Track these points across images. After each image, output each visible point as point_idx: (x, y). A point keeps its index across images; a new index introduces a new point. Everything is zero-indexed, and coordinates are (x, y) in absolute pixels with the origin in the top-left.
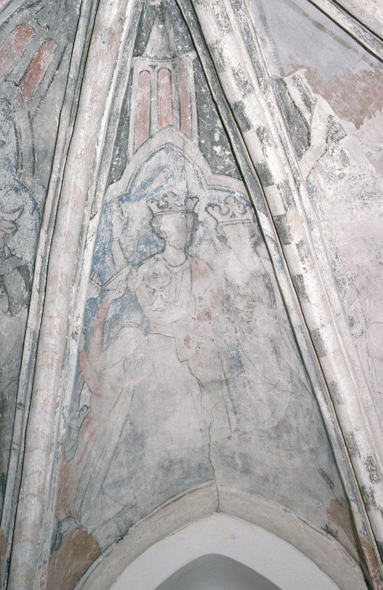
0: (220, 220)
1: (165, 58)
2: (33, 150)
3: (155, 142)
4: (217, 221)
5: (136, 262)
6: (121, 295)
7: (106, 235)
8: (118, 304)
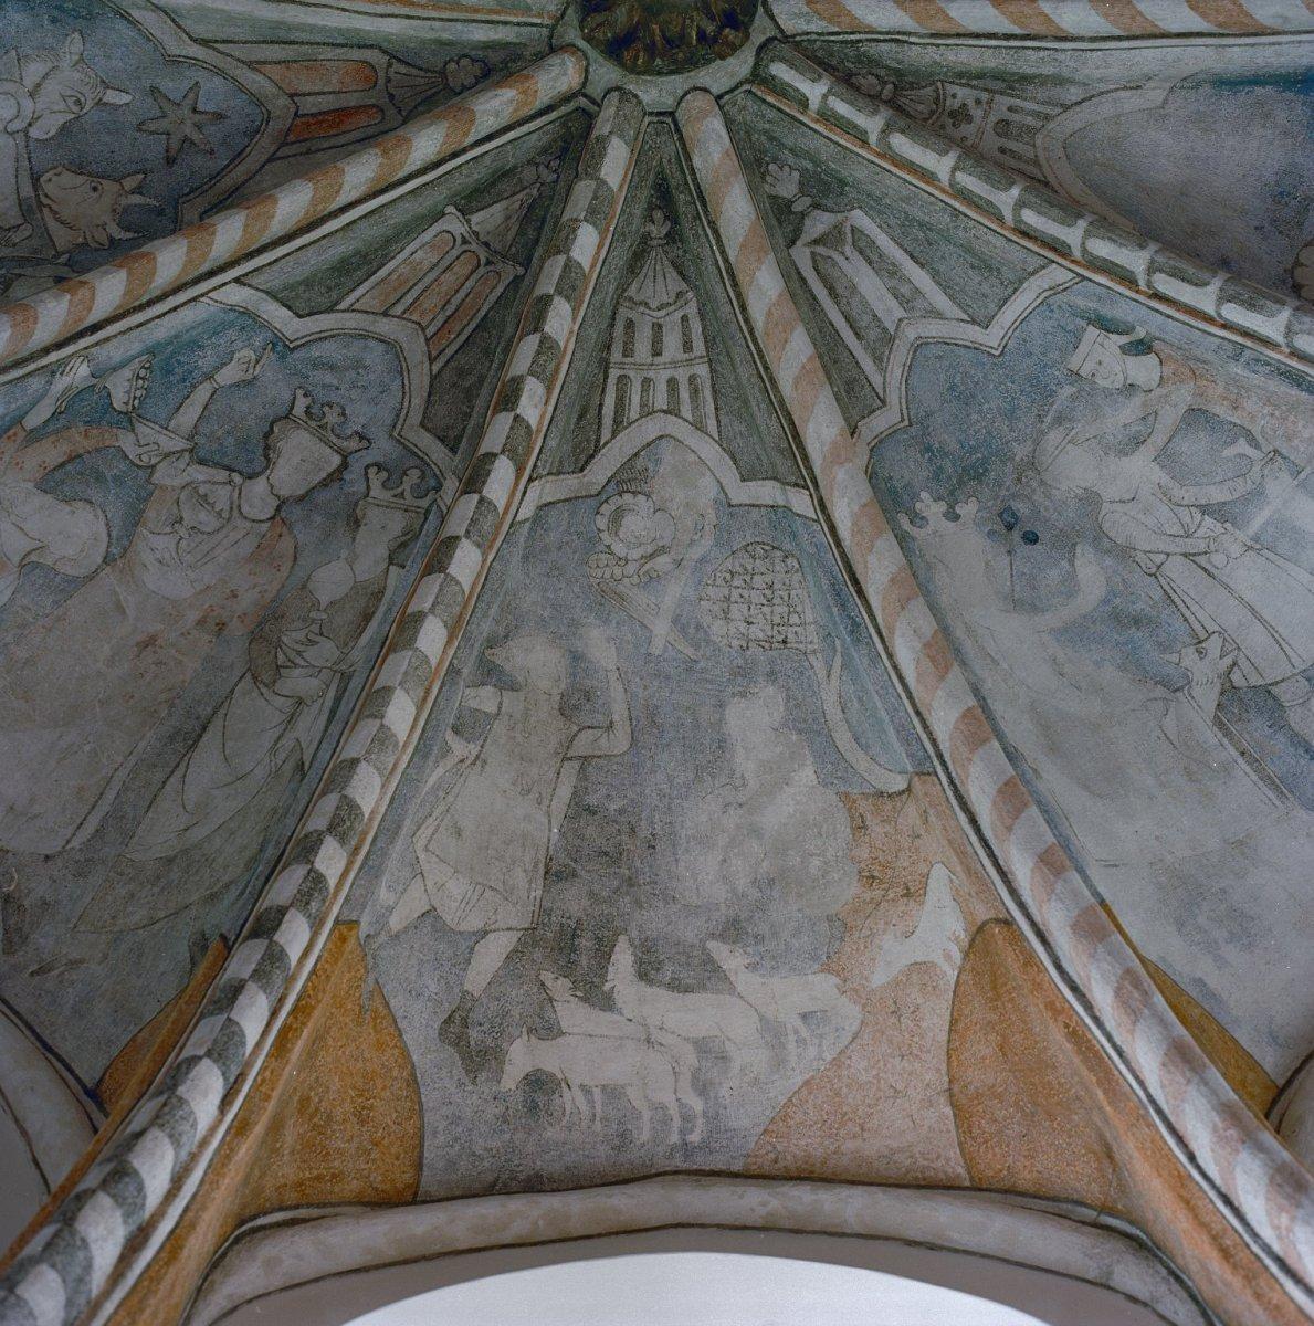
0: (372, 493)
1: (486, 244)
3: (385, 327)
4: (368, 495)
5: (202, 454)
6: (137, 461)
7: (206, 360)
8: (122, 466)
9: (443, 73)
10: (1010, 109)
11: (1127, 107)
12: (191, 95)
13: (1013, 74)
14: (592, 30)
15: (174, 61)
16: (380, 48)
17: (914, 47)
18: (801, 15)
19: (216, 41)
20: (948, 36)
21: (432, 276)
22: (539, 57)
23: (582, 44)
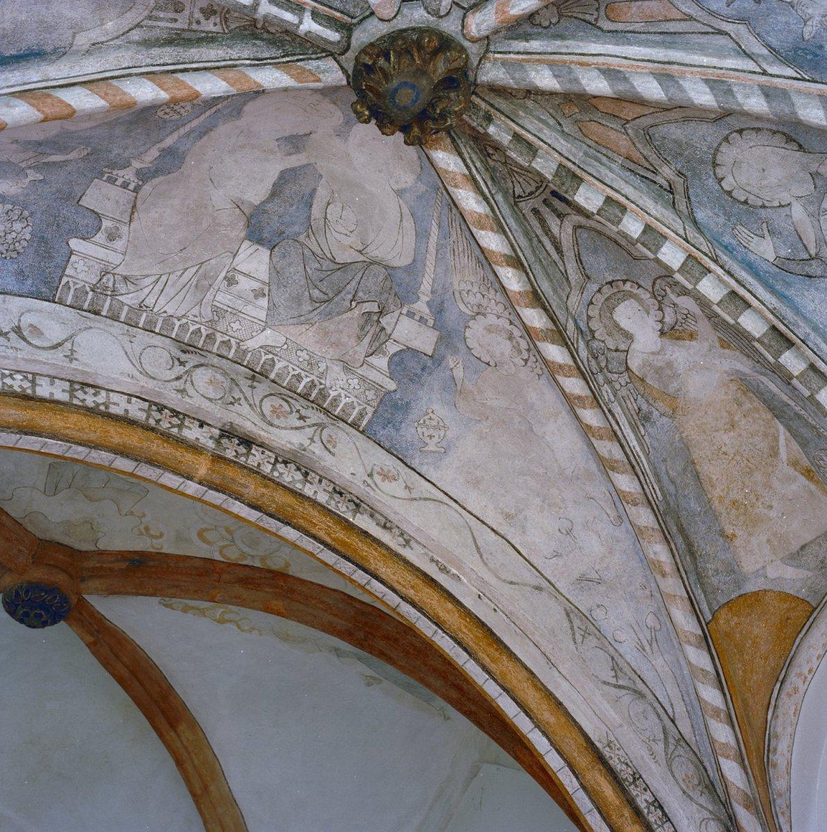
9: (560, 16)
10: (176, 20)
11: (98, 31)
13: (178, 45)
14: (460, 57)
15: (742, 20)
16: (602, 30)
17: (246, 57)
18: (323, 72)
19: (713, 33)
20: (224, 67)
22: (496, 32)
23: (466, 44)
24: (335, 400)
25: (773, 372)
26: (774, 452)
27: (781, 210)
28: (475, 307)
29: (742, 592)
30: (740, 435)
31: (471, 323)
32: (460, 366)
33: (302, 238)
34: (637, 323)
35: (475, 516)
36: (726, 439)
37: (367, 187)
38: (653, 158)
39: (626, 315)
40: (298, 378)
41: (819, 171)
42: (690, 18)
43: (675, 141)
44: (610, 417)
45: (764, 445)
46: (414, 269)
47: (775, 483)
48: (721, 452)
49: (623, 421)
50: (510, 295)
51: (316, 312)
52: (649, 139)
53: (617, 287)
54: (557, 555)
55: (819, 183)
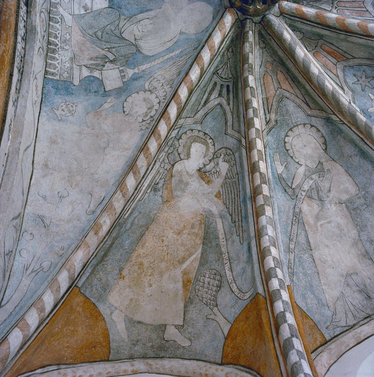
1: (332, 3)
2: (368, 59)
12: (356, 83)
15: (352, 91)
19: (340, 86)
21: (349, 8)
24: (54, 58)
25: (231, 215)
26: (182, 261)
27: (297, 164)
28: (153, 88)
29: (97, 304)
30: (177, 240)
31: (140, 93)
32: (111, 104)
33: (123, 17)
34: (197, 156)
35: (34, 150)
36: (170, 235)
37: (172, 24)
38: (274, 107)
39: (197, 149)
40: (56, 37)
41: (323, 163)
42: (338, 77)
43: (287, 110)
44: (153, 162)
45: (181, 254)
46: (147, 58)
47: (166, 276)
48: (162, 238)
49: (154, 172)
50: (188, 77)
51: (90, 37)
52: (280, 100)
53: (206, 137)
54: (44, 198)
55: (319, 167)
